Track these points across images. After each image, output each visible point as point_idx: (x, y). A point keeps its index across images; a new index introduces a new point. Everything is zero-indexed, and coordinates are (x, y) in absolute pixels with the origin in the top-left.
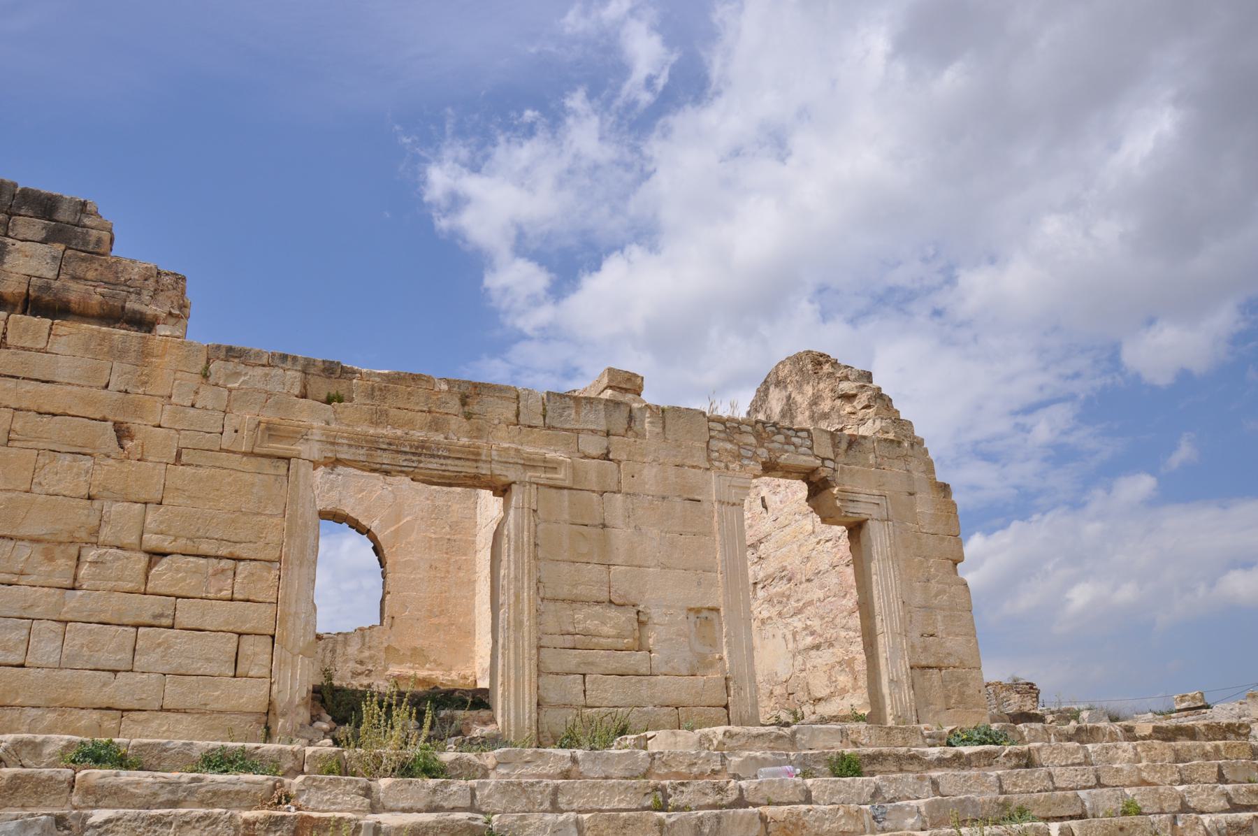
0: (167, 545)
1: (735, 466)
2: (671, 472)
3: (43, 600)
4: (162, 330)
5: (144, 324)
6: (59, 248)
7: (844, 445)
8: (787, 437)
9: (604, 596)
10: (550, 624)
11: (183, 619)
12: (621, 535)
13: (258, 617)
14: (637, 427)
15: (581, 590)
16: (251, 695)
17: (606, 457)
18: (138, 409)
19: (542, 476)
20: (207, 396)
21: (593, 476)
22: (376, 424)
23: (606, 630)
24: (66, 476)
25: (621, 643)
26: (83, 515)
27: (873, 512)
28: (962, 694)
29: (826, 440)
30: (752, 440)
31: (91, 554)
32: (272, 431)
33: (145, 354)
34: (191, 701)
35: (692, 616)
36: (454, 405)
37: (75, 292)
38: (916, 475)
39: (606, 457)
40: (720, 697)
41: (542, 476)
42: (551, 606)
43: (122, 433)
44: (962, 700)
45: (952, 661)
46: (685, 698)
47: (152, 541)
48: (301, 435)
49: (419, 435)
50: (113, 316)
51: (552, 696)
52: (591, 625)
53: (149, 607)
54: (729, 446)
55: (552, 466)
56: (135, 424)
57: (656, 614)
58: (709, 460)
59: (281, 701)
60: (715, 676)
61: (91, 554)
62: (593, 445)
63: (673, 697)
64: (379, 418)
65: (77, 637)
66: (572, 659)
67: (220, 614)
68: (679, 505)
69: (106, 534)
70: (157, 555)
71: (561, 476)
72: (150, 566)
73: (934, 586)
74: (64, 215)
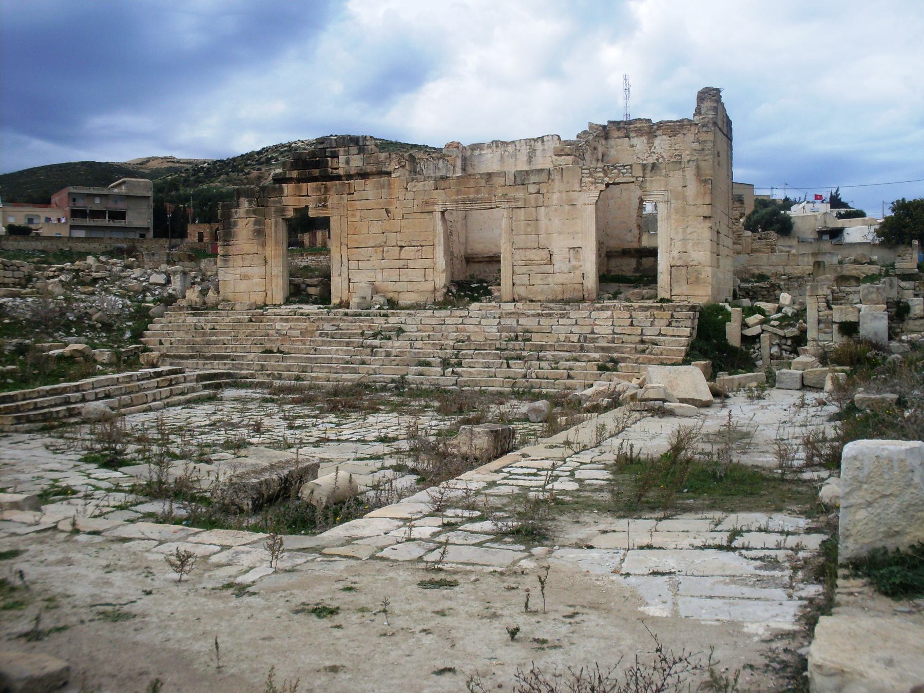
0: (403, 244)
1: (592, 187)
2: (564, 194)
3: (377, 263)
4: (393, 175)
5: (389, 174)
6: (361, 156)
7: (649, 168)
8: (619, 170)
9: (536, 246)
10: (517, 257)
11: (411, 266)
12: (543, 222)
13: (428, 263)
14: (552, 177)
15: (529, 245)
16: (429, 286)
17: (538, 193)
18: (390, 203)
19: (513, 204)
20: (410, 195)
21: (533, 202)
22: (458, 195)
23: (536, 258)
24: (376, 228)
25: (542, 262)
26: (381, 239)
27: (660, 198)
28: (697, 278)
29: (640, 168)
30: (602, 175)
31: (386, 249)
32: (427, 204)
33: (389, 185)
34: (415, 289)
35: (572, 251)
36: (483, 182)
37: (369, 169)
38: (688, 177)
39: (538, 193)
40: (581, 280)
41: (513, 204)
42: (518, 251)
43: (387, 211)
44: (697, 281)
45: (694, 263)
46: (565, 281)
47: (400, 243)
48: (434, 204)
49: (472, 196)
50: (381, 173)
51: (517, 282)
52: (532, 257)
53: (401, 263)
54: (590, 179)
55: (515, 200)
56: (391, 208)
57: (555, 251)
58: (581, 187)
59: (437, 287)
60: (578, 273)
61: (386, 249)
62: (532, 189)
63: (560, 281)
64: (458, 193)
65: (386, 273)
66: (524, 269)
67: (419, 263)
68: (567, 208)
69: (388, 244)
70: (402, 247)
71: (520, 204)
72: (401, 250)
73: (689, 230)
74: (361, 143)
